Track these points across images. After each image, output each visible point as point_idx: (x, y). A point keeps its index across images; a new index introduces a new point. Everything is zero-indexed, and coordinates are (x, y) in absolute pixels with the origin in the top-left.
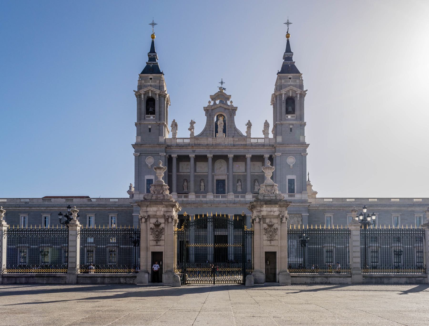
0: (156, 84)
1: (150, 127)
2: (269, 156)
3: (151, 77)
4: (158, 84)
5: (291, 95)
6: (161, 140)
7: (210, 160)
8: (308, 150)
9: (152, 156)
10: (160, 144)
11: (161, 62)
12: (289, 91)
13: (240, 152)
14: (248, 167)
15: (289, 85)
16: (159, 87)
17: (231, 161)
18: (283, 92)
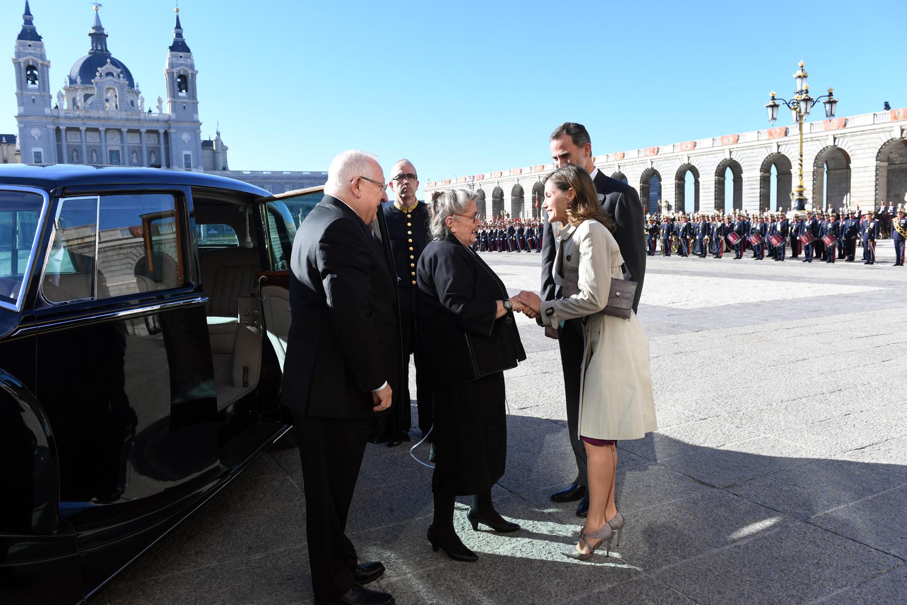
0: (37, 52)
1: (33, 98)
2: (163, 131)
3: (30, 44)
4: (39, 52)
5: (182, 74)
6: (47, 111)
7: (103, 133)
8: (201, 127)
9: (38, 127)
10: (46, 116)
11: (39, 26)
12: (180, 70)
13: (135, 125)
14: (144, 141)
15: (181, 64)
16: (41, 55)
17: (125, 134)
18: (175, 70)
